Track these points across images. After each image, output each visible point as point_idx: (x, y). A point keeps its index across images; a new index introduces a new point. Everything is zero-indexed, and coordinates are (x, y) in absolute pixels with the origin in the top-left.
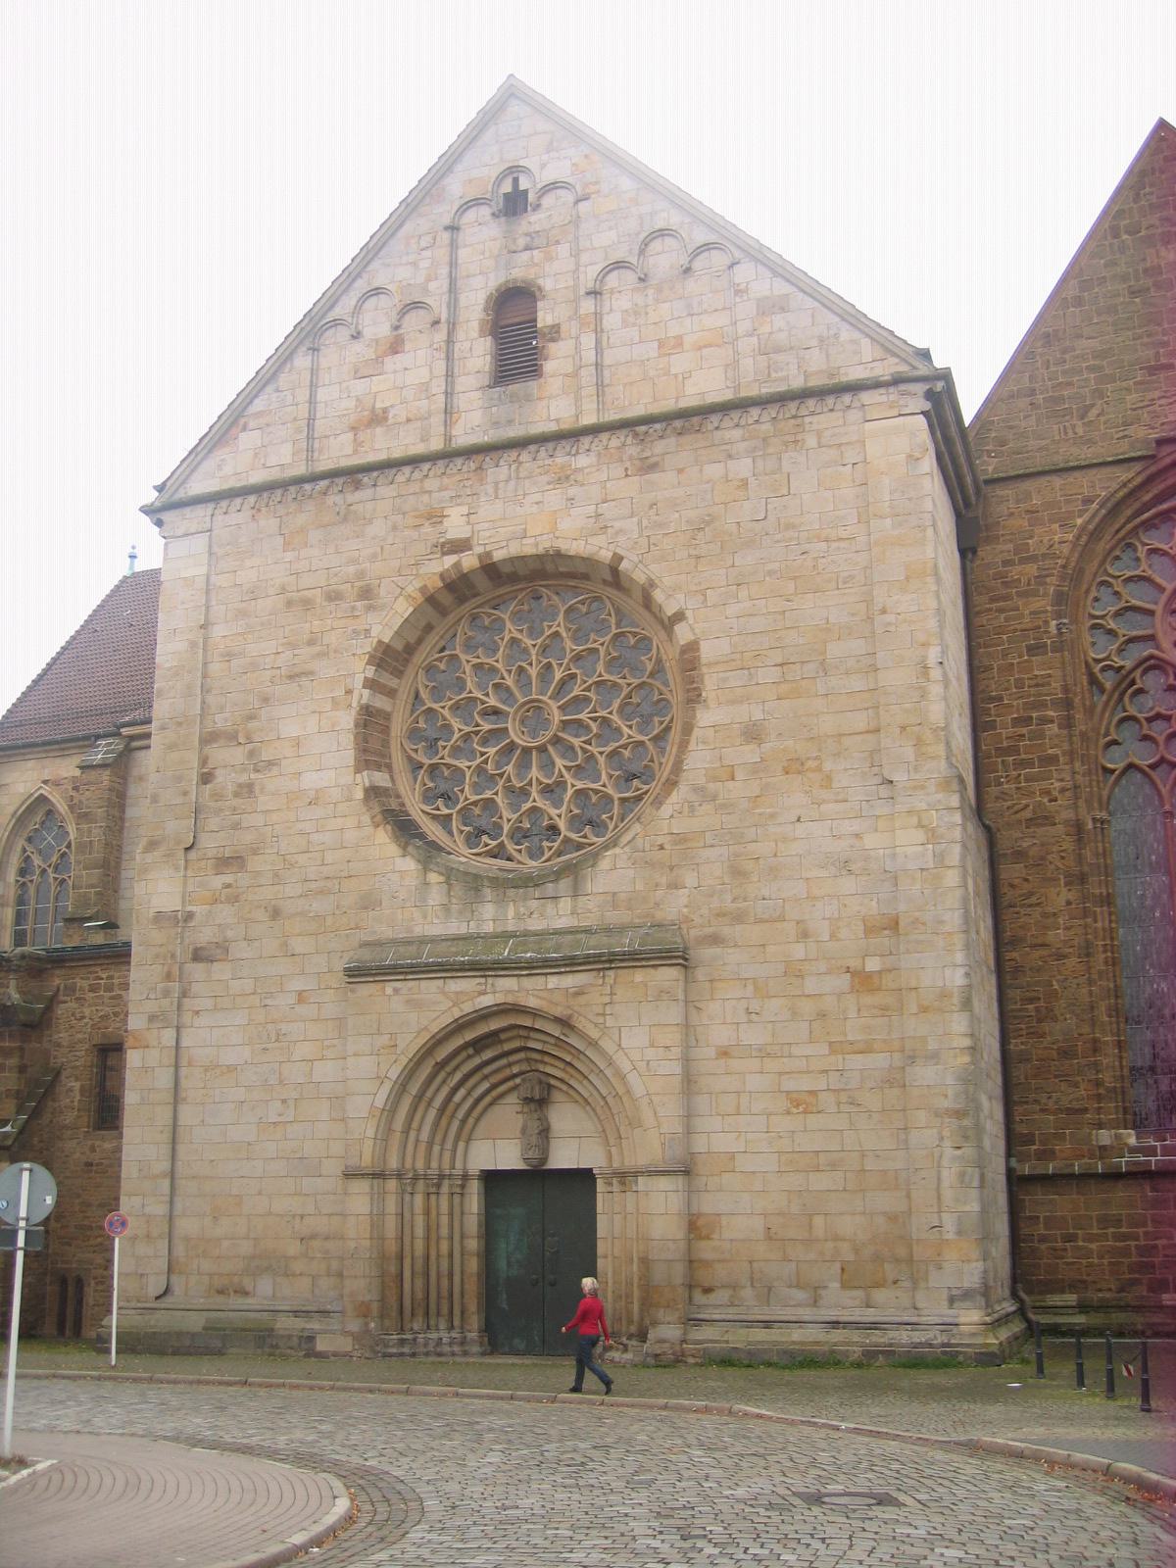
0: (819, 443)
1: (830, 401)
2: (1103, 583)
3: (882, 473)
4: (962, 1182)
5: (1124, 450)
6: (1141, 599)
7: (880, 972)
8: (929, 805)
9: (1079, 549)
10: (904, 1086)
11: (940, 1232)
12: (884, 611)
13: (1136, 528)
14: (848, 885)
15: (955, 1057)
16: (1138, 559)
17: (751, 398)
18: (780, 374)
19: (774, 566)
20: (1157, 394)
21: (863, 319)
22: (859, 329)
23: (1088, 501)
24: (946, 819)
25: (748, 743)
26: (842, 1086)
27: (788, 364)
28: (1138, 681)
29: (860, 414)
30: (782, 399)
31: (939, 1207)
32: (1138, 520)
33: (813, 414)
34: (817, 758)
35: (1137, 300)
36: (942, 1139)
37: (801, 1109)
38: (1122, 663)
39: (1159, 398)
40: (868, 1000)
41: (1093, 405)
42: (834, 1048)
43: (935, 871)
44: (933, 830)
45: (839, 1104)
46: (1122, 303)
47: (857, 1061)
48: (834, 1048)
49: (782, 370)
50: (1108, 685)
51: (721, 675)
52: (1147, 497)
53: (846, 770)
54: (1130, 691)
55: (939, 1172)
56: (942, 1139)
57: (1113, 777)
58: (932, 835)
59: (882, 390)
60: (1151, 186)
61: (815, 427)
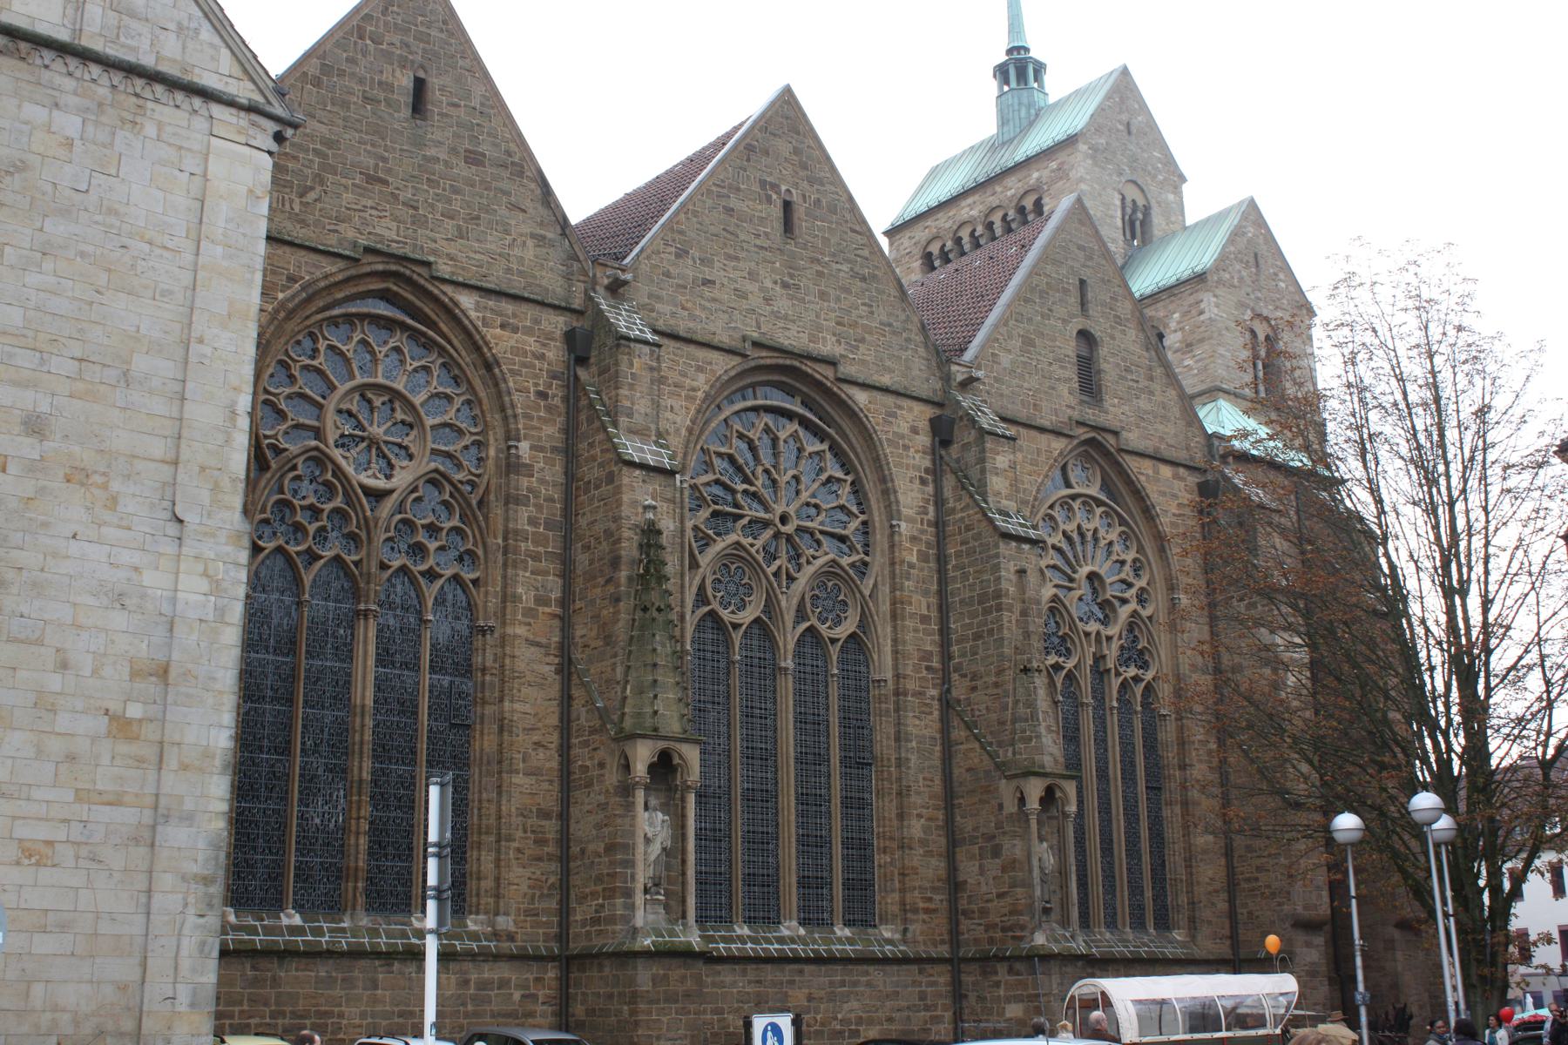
0: (158, 136)
1: (179, 96)
2: (281, 362)
3: (221, 197)
4: (201, 951)
5: (331, 242)
6: (311, 388)
7: (140, 721)
8: (217, 555)
9: (276, 322)
10: (152, 845)
11: (173, 1004)
12: (201, 341)
13: (323, 320)
14: (119, 620)
15: (210, 821)
16: (315, 351)
17: (96, 53)
18: (129, 42)
19: (90, 249)
20: (370, 203)
21: (229, 28)
22: (221, 37)
23: (292, 279)
24: (232, 574)
25: (28, 435)
26: (83, 840)
27: (140, 35)
28: (300, 466)
29: (205, 125)
30: (132, 70)
31: (175, 978)
32: (328, 314)
33: (157, 101)
34: (104, 474)
35: (369, 107)
36: (186, 905)
37: (33, 860)
38: (287, 446)
39: (372, 208)
40: (123, 748)
41: (312, 188)
42: (81, 796)
43: (213, 625)
44: (217, 581)
45: (77, 858)
46: (355, 103)
47: (104, 814)
48: (81, 796)
49: (133, 38)
50: (274, 465)
51: (7, 348)
52: (340, 295)
53: (134, 495)
54: (291, 475)
55: (179, 940)
56: (186, 905)
57: (262, 555)
58: (216, 587)
59: (234, 111)
60: (399, 6)
61: (156, 116)
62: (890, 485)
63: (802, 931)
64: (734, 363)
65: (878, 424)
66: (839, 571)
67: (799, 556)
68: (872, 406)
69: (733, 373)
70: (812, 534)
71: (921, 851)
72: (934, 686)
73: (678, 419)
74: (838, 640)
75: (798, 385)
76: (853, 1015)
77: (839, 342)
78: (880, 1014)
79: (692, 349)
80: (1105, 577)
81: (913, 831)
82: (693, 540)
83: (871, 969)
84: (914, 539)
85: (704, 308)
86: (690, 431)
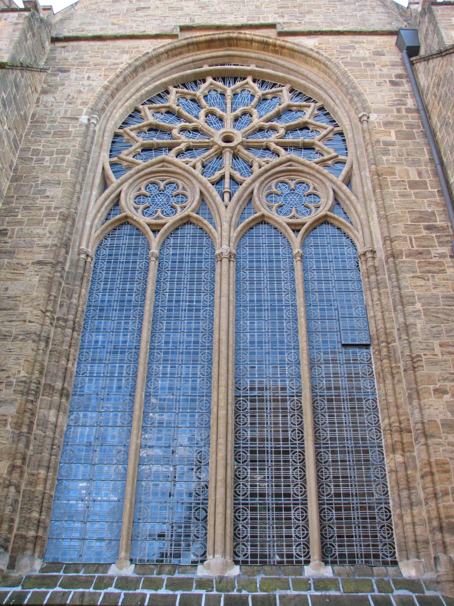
62: (351, 91)
63: (236, 571)
64: (162, 44)
65: (332, 55)
67: (251, 167)
68: (324, 46)
69: (162, 50)
70: (267, 148)
72: (442, 244)
73: (94, 83)
74: (303, 224)
75: (245, 54)
77: (283, 17)
79: (120, 43)
81: (432, 411)
82: (108, 167)
84: (387, 124)
85: (136, 21)
86: (106, 88)
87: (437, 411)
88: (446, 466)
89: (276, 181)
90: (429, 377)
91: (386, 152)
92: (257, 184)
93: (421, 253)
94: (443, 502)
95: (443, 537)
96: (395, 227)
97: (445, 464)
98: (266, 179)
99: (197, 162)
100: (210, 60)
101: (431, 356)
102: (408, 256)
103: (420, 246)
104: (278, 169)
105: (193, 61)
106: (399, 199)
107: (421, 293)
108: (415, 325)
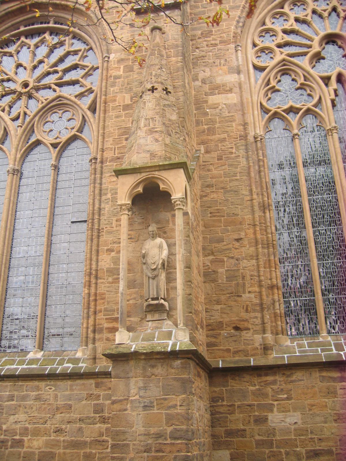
66: (66, 101)
71: (110, 279)
76: (18, 426)
78: (48, 426)
80: (341, 33)
83: (42, 384)
87: (106, 263)
88: (104, 296)
89: (51, 113)
90: (106, 241)
91: (113, 85)
92: (37, 118)
93: (119, 158)
94: (98, 316)
95: (95, 335)
96: (107, 141)
97: (103, 294)
98: (44, 113)
99: (6, 105)
100: (24, 22)
101: (109, 228)
102: (110, 162)
103: (119, 153)
104: (51, 104)
105: (12, 25)
106: (114, 120)
107: (113, 187)
108: (105, 208)
